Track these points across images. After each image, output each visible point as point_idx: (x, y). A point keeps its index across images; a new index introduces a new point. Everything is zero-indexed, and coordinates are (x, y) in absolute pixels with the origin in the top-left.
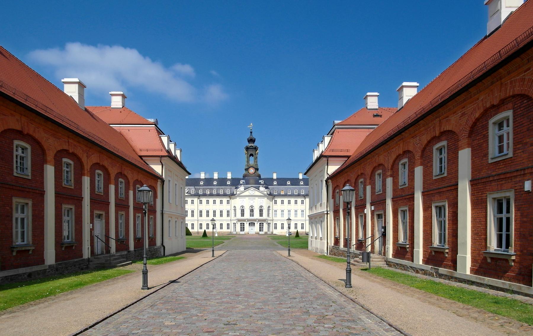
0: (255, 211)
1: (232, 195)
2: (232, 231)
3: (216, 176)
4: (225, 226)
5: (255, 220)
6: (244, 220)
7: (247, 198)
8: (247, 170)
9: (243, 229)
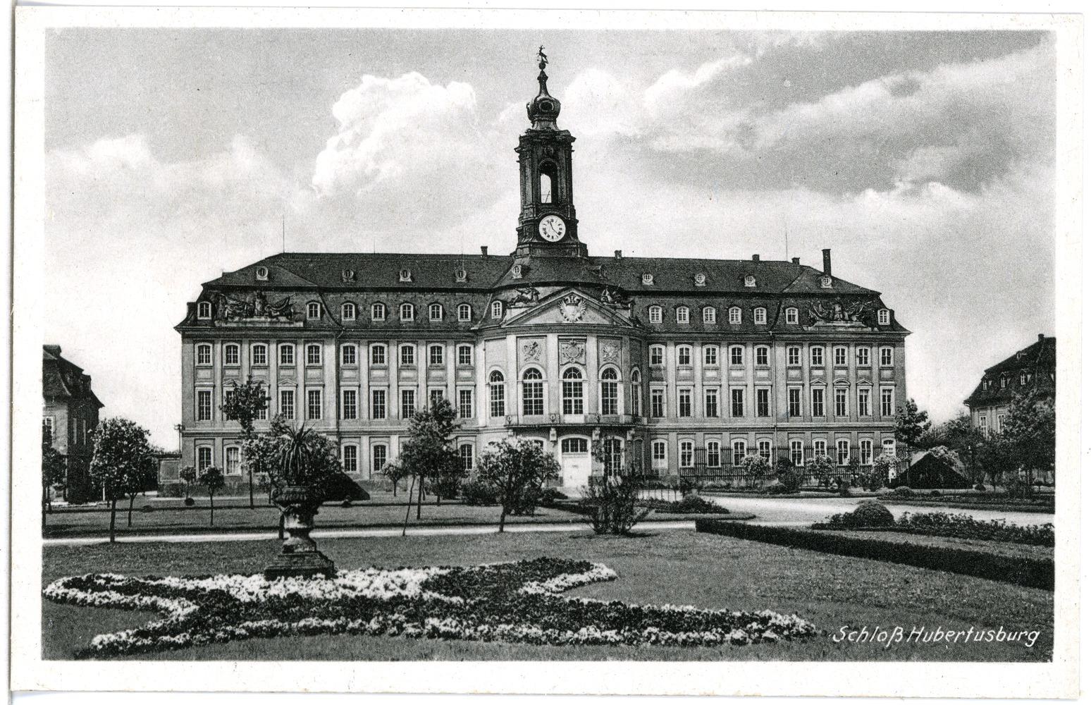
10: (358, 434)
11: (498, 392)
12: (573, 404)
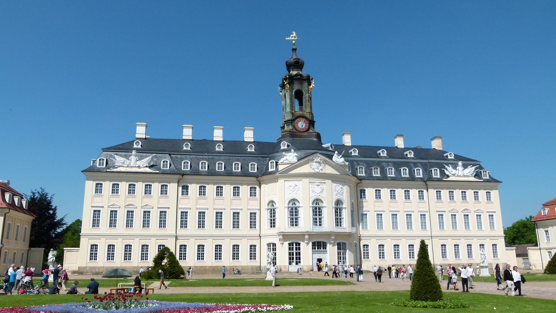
0: (325, 212)
1: (262, 176)
2: (264, 263)
3: (218, 135)
4: (244, 252)
5: (328, 235)
6: (301, 236)
7: (306, 180)
8: (291, 122)
9: (295, 256)
10: (188, 237)
11: (273, 213)
12: (318, 220)
